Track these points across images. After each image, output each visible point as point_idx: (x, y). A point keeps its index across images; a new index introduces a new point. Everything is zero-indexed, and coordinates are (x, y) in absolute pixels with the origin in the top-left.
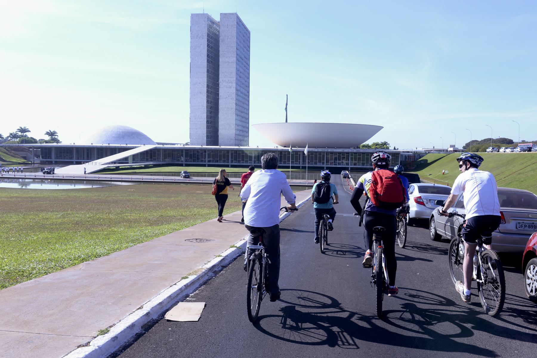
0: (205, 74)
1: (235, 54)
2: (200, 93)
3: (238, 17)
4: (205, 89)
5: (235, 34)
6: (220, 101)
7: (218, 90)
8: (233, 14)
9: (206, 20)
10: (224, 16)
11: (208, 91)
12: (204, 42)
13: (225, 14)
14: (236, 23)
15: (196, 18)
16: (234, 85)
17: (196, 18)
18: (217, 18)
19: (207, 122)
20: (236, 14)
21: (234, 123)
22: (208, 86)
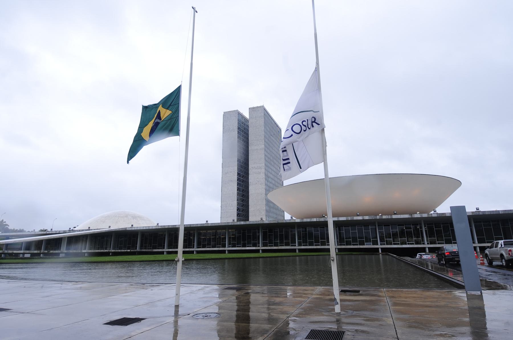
1: (264, 141)
2: (231, 181)
3: (265, 110)
4: (236, 177)
5: (263, 124)
6: (250, 188)
7: (248, 178)
8: (260, 107)
10: (252, 110)
11: (238, 179)
12: (235, 133)
13: (253, 108)
14: (263, 115)
15: (227, 115)
16: (263, 170)
17: (227, 115)
18: (247, 115)
20: (263, 106)
21: (265, 208)
22: (238, 174)
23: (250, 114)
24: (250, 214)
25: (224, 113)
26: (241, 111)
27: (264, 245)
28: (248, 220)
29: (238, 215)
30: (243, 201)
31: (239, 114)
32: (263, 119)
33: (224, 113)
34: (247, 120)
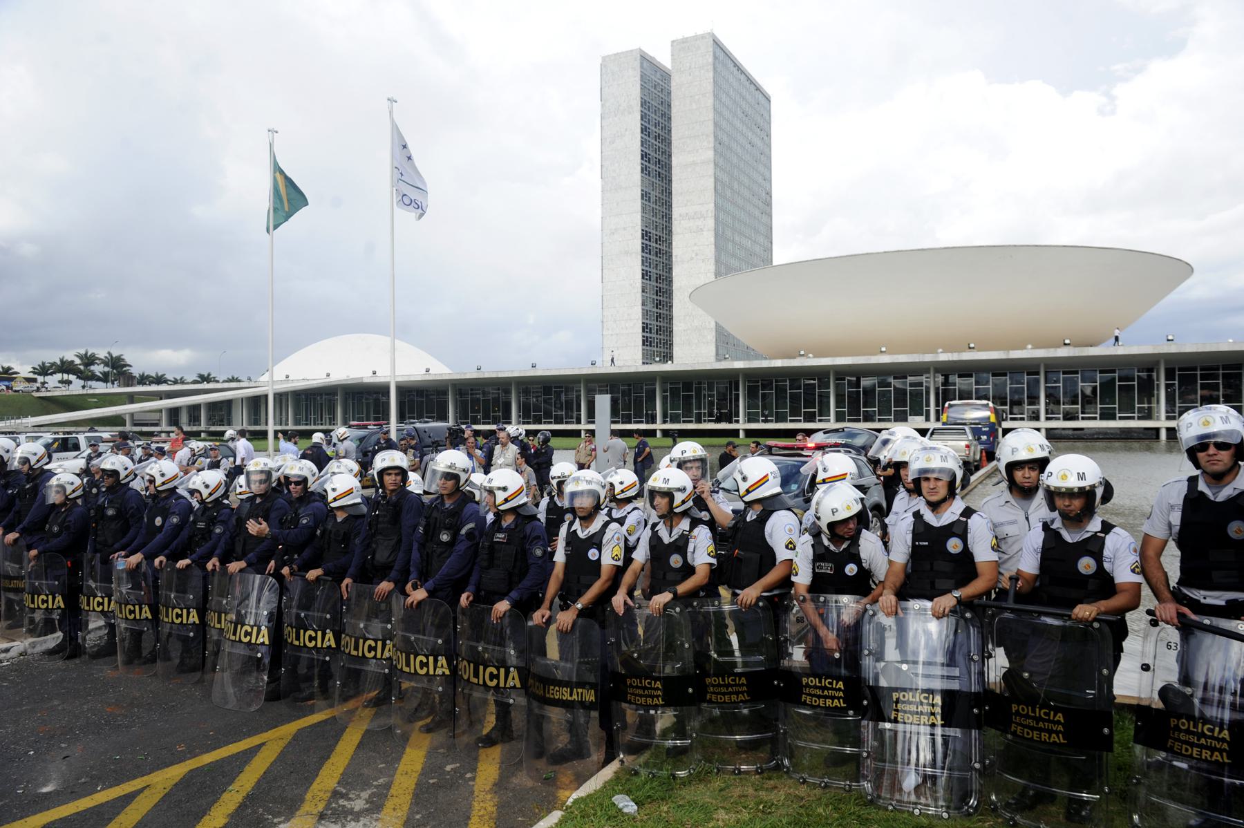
0: (637, 204)
1: (712, 139)
2: (626, 253)
3: (717, 43)
4: (637, 243)
5: (709, 87)
8: (703, 37)
9: (637, 64)
10: (681, 46)
11: (645, 248)
12: (633, 123)
13: (684, 41)
14: (711, 60)
15: (610, 66)
16: (711, 223)
17: (610, 66)
18: (664, 58)
19: (645, 328)
22: (645, 235)
23: (673, 60)
24: (676, 339)
25: (604, 59)
26: (651, 52)
27: (751, 418)
28: (668, 357)
29: (646, 342)
30: (658, 304)
31: (645, 59)
32: (711, 74)
33: (604, 59)
34: (666, 76)
